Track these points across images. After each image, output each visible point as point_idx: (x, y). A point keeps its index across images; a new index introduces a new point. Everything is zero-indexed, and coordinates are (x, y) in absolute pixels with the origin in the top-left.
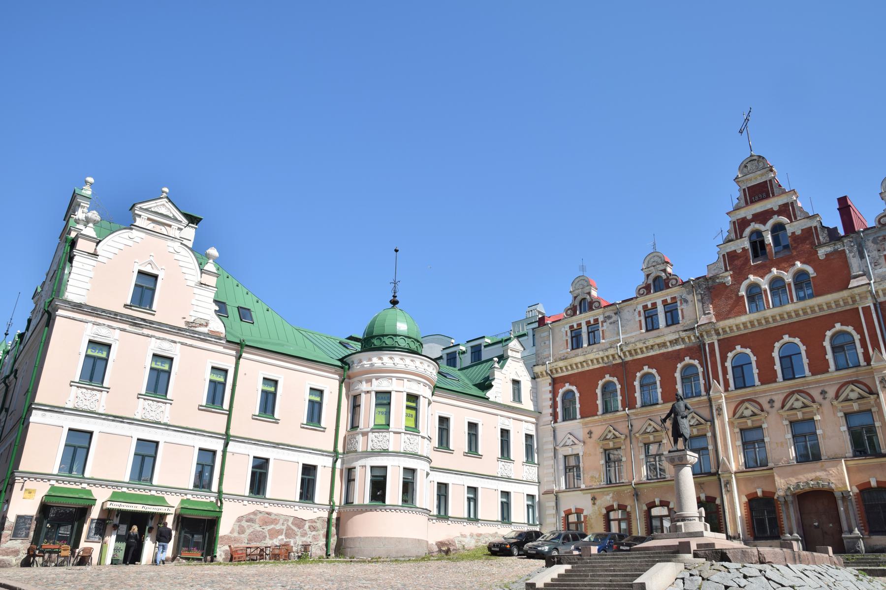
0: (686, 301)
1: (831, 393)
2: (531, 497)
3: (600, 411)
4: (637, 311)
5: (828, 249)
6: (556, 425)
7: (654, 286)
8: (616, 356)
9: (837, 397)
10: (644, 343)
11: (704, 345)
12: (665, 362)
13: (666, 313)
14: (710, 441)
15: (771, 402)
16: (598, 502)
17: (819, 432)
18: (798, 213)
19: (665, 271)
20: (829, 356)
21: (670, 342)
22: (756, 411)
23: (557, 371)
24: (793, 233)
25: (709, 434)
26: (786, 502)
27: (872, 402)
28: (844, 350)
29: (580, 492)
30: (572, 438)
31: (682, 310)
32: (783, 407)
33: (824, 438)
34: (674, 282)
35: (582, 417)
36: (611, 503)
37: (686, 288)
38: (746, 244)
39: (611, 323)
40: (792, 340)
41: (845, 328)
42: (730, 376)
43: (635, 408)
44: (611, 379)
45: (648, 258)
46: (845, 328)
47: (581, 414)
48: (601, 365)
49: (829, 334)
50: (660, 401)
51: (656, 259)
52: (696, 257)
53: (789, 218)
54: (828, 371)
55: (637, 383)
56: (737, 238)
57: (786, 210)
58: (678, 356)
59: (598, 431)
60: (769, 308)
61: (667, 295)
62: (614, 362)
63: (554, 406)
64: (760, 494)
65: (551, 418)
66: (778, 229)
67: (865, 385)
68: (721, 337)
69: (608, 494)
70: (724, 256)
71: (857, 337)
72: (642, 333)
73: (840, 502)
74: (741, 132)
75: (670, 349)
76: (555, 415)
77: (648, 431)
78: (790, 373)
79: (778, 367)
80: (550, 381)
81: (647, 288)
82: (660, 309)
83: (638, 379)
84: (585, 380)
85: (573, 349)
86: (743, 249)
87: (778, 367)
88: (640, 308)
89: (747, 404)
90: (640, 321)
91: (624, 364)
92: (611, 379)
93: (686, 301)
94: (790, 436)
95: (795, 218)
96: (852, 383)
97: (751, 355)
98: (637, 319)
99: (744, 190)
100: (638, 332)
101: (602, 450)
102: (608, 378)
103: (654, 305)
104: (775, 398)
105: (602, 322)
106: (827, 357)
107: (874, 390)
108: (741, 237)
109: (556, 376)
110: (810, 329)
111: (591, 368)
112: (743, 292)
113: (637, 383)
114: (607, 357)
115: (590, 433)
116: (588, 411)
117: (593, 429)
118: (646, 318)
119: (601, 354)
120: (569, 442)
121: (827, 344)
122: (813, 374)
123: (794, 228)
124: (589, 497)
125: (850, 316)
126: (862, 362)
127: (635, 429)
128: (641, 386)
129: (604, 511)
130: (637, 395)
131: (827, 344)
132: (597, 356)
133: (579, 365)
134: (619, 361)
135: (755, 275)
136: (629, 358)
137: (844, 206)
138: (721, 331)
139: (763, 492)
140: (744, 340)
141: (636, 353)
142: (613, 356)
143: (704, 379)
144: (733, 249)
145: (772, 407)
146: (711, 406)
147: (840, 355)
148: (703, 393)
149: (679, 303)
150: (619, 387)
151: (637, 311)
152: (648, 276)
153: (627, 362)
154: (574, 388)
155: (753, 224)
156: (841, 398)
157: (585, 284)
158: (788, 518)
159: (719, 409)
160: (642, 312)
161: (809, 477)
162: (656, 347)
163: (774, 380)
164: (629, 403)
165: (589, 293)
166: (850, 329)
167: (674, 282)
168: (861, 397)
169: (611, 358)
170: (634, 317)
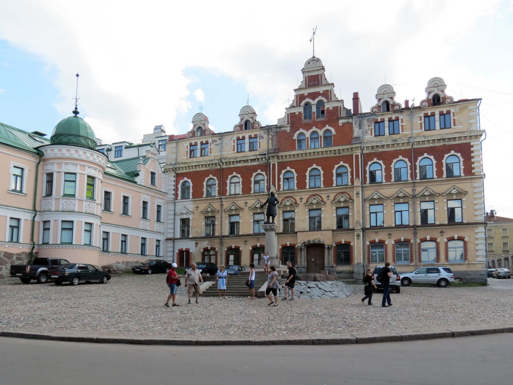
0: (262, 138)
1: (332, 197)
4: (233, 139)
5: (345, 121)
8: (218, 164)
10: (235, 159)
11: (270, 164)
12: (246, 173)
13: (250, 143)
15: (301, 199)
18: (333, 97)
20: (334, 178)
21: (251, 160)
24: (328, 108)
26: (301, 249)
28: (342, 176)
31: (260, 142)
32: (307, 202)
33: (324, 219)
34: (257, 125)
37: (264, 130)
38: (301, 110)
39: (216, 145)
40: (317, 167)
41: (345, 164)
43: (225, 195)
46: (345, 164)
48: (208, 168)
52: (273, 113)
53: (327, 99)
54: (332, 186)
57: (328, 95)
58: (254, 169)
61: (252, 132)
62: (216, 168)
64: (288, 245)
66: (320, 104)
68: (280, 161)
70: (288, 115)
73: (326, 251)
74: (311, 41)
75: (250, 164)
77: (232, 208)
81: (240, 126)
82: (247, 140)
84: (197, 177)
86: (300, 112)
88: (235, 138)
90: (234, 146)
91: (222, 170)
93: (262, 138)
95: (331, 100)
96: (342, 193)
97: (295, 173)
98: (233, 144)
99: (306, 77)
100: (233, 152)
102: (211, 176)
103: (244, 138)
104: (303, 197)
108: (300, 106)
110: (327, 164)
111: (201, 169)
113: (228, 181)
114: (212, 164)
118: (238, 145)
119: (209, 163)
122: (325, 187)
123: (329, 106)
125: (348, 159)
126: (350, 184)
127: (225, 207)
128: (231, 183)
130: (228, 188)
131: (334, 171)
134: (219, 167)
135: (303, 129)
136: (225, 166)
137: (356, 98)
138: (280, 157)
139: (290, 244)
140: (292, 164)
142: (216, 164)
143: (267, 183)
147: (339, 179)
148: (266, 191)
149: (258, 138)
151: (233, 139)
152: (242, 119)
153: (223, 169)
155: (307, 99)
158: (301, 257)
160: (236, 140)
161: (314, 237)
166: (347, 165)
167: (257, 125)
168: (345, 201)
169: (214, 165)
170: (230, 143)
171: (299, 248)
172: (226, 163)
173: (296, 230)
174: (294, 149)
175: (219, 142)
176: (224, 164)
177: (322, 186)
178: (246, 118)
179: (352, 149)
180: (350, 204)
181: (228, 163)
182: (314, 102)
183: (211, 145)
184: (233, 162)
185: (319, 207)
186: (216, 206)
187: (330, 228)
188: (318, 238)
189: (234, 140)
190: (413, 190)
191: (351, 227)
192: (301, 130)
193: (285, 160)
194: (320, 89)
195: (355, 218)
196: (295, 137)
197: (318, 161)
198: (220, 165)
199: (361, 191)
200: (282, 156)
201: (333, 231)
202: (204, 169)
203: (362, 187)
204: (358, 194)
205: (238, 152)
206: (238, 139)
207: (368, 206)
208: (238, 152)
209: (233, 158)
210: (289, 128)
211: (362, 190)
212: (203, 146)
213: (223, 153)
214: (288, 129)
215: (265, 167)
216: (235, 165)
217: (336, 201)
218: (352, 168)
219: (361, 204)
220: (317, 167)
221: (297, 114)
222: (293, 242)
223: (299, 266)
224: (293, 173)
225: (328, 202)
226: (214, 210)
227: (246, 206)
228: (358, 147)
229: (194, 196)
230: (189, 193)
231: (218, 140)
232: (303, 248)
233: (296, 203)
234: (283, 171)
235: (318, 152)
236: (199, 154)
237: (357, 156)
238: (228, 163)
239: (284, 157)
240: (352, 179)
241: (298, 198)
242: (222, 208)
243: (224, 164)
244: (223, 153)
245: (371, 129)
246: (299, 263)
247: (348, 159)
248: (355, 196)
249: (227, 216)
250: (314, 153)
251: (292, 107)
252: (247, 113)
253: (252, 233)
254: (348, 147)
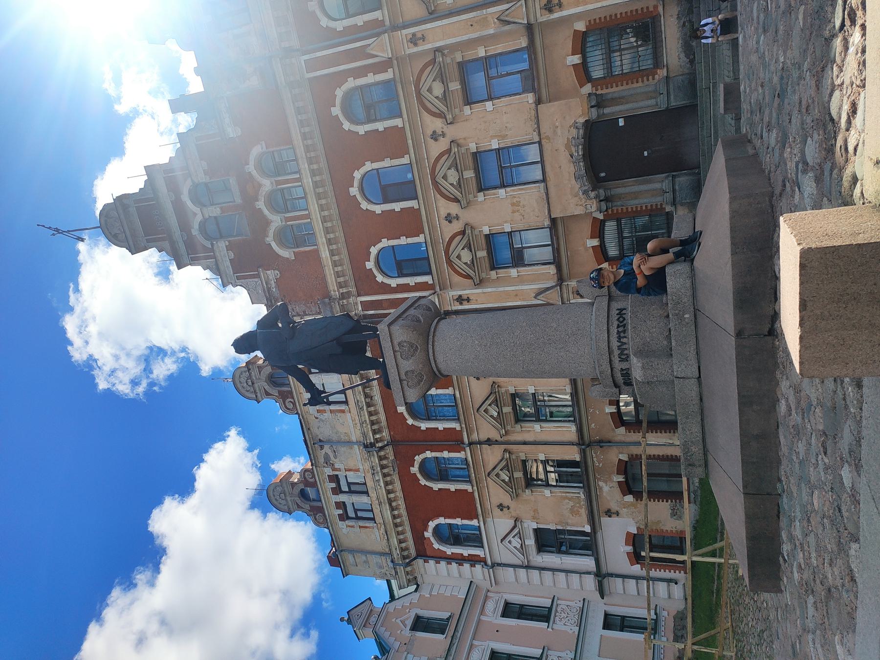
1: (437, 124)
2: (609, 622)
3: (468, 487)
6: (489, 562)
7: (283, 385)
8: (382, 453)
9: (441, 115)
10: (362, 409)
16: (614, 507)
17: (495, 146)
19: (260, 368)
22: (464, 242)
23: (407, 549)
26: (607, 199)
27: (448, 60)
29: (599, 535)
30: (510, 537)
32: (456, 200)
33: (504, 137)
35: (476, 517)
36: (616, 485)
38: (222, 245)
40: (356, 183)
42: (411, 281)
43: (461, 431)
44: (417, 465)
45: (243, 391)
47: (471, 519)
49: (347, 126)
50: (450, 391)
51: (243, 380)
55: (424, 426)
56: (214, 257)
59: (496, 493)
60: (308, 216)
62: (392, 457)
63: (460, 560)
65: (478, 567)
67: (422, 71)
68: (353, 290)
69: (601, 488)
70: (238, 278)
71: (351, 83)
76: (473, 560)
77: (495, 414)
78: (406, 190)
79: (397, 207)
80: (420, 561)
83: (416, 424)
84: (420, 506)
85: (373, 519)
86: (228, 248)
87: (397, 207)
88: (312, 409)
89: (453, 258)
92: (417, 465)
94: (502, 192)
102: (415, 470)
104: (443, 213)
105: (334, 469)
106: (381, 129)
107: (431, 57)
108: (212, 250)
109: (413, 552)
111: (400, 494)
113: (424, 426)
114: (383, 467)
115: (501, 507)
116: (465, 505)
117: (495, 501)
119: (379, 477)
120: (516, 542)
121: (361, 130)
124: (605, 520)
127: (494, 435)
128: (429, 419)
129: (630, 498)
130: (441, 426)
132: (382, 485)
133: (396, 512)
134: (389, 451)
136: (385, 434)
140: (358, 257)
141: (378, 422)
142: (381, 458)
145: (457, 217)
146: (457, 312)
150: (429, 454)
152: (268, 394)
154: (432, 525)
156: (443, 108)
157: (279, 489)
158: (636, 195)
159: (460, 299)
160: (318, 407)
162: (367, 390)
163: (414, 213)
164: (453, 441)
165: (293, 484)
168: (442, 77)
169: (385, 462)
171: (604, 206)
172: (375, 432)
173: (547, 223)
174: (315, 255)
175: (327, 449)
176: (378, 436)
177: (405, 160)
178: (262, 384)
180: (448, 60)
181: (375, 427)
183: (339, 470)
184: (370, 414)
185: (470, 161)
186: (492, 456)
187: (533, 112)
188: (567, 147)
189: (318, 411)
191: (523, 43)
192: (270, 239)
195: (492, 31)
198: (382, 448)
199: (405, 32)
200: (340, 285)
201: (539, 102)
202: (398, 486)
203: (395, 28)
204: (414, 40)
205: (346, 402)
208: (346, 402)
209: (360, 416)
210: (269, 272)
211: (405, 27)
212: (345, 488)
214: (272, 274)
216: (381, 409)
217: (443, 108)
218: (342, 77)
219: (445, 22)
220: (356, 183)
221: (232, 256)
222: (586, 227)
223: (669, 196)
225: (453, 132)
226: (503, 463)
229: (471, 514)
230: (464, 527)
231: (323, 452)
232: (601, 191)
233: (463, 233)
234: (380, 278)
235: (316, 185)
236: (364, 499)
238: (375, 427)
239: (341, 279)
242: (497, 442)
243: (378, 436)
244: (354, 439)
246: (658, 200)
249: (518, 427)
250: (319, 197)
251: (217, 270)
252: (250, 383)
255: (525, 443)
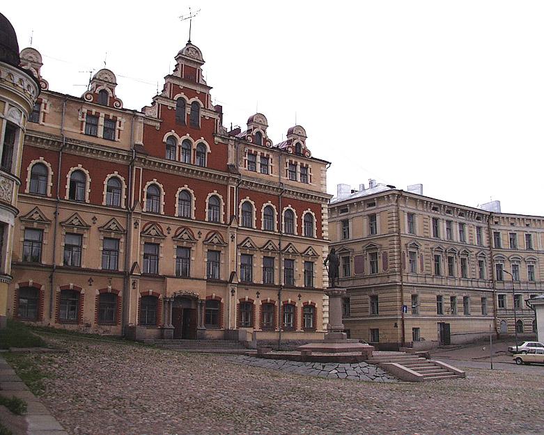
14: (122, 245)
25: (122, 240)
32: (176, 236)
38: (175, 106)
57: (205, 97)
58: (112, 167)
72: (81, 133)
75: (104, 158)
88: (85, 110)
100: (79, 132)
101: (23, 228)
112: (165, 140)
144: (166, 103)
159: (136, 224)
168: (219, 244)
179: (228, 178)
182: (190, 102)
185: (189, 245)
186: (48, 212)
190: (279, 244)
193: (151, 168)
194: (199, 89)
196: (165, 140)
197: (192, 182)
206: (89, 114)
207: (239, 254)
213: (65, 128)
215: (126, 171)
218: (226, 201)
222: (158, 291)
224: (159, 189)
227: (94, 223)
228: (235, 178)
237: (232, 188)
240: (225, 216)
241: (164, 227)
245: (245, 160)
247: (223, 189)
248: (230, 239)
253: (100, 268)
254: (226, 175)
255: (55, 235)
